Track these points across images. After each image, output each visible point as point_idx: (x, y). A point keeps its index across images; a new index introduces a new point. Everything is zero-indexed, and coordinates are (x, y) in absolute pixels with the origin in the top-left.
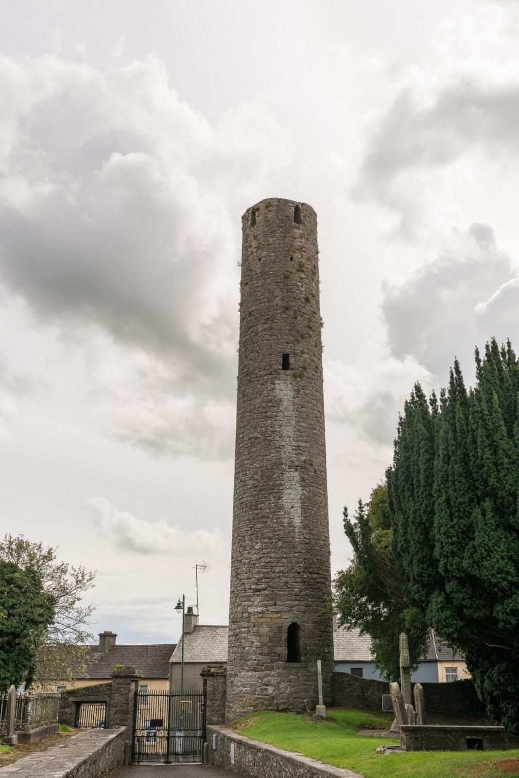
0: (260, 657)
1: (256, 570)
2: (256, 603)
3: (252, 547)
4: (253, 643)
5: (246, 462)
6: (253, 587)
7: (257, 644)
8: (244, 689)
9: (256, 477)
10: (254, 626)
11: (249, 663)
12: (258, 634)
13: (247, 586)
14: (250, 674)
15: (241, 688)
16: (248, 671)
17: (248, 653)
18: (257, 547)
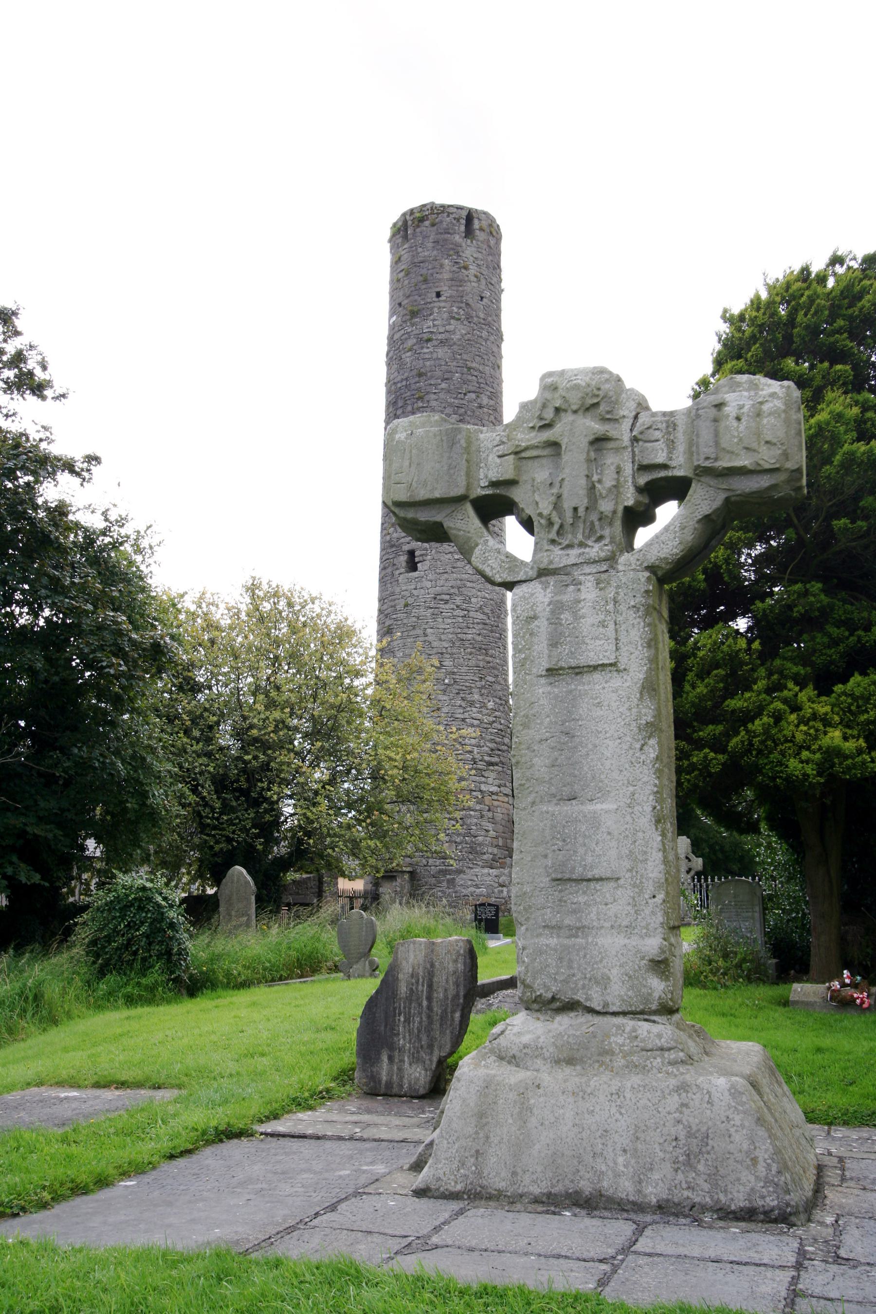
0: (495, 851)
1: (489, 737)
2: (490, 780)
3: (484, 706)
4: (487, 831)
5: (469, 584)
6: (487, 758)
7: (492, 833)
8: (478, 891)
9: (486, 610)
10: (489, 810)
11: (485, 857)
12: (492, 820)
13: (478, 756)
14: (486, 870)
15: (472, 889)
16: (483, 867)
17: (480, 845)
18: (491, 705)
